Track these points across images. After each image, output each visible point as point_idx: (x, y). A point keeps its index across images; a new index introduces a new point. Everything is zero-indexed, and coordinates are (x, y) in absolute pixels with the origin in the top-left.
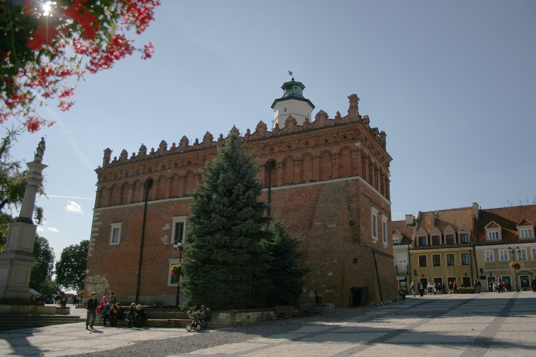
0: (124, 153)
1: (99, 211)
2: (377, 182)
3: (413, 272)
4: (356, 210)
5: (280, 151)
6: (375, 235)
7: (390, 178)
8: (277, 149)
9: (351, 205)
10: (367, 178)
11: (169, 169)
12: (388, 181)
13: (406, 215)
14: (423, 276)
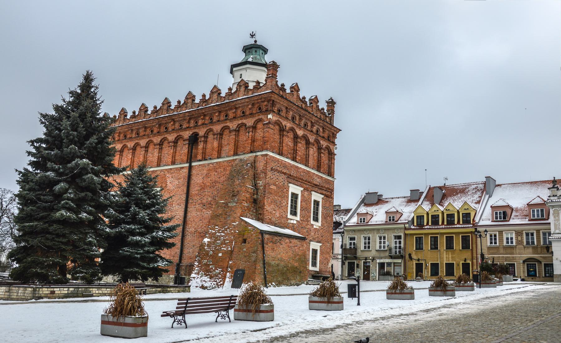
3: (407, 257)
4: (262, 187)
5: (203, 124)
9: (258, 182)
13: (411, 191)
14: (419, 260)
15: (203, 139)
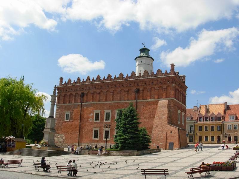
0: (70, 81)
1: (59, 106)
2: (181, 98)
3: (195, 134)
5: (141, 85)
6: (179, 121)
7: (186, 96)
8: (140, 84)
9: (170, 110)
10: (177, 98)
11: (92, 89)
12: (185, 97)
15: (142, 91)
